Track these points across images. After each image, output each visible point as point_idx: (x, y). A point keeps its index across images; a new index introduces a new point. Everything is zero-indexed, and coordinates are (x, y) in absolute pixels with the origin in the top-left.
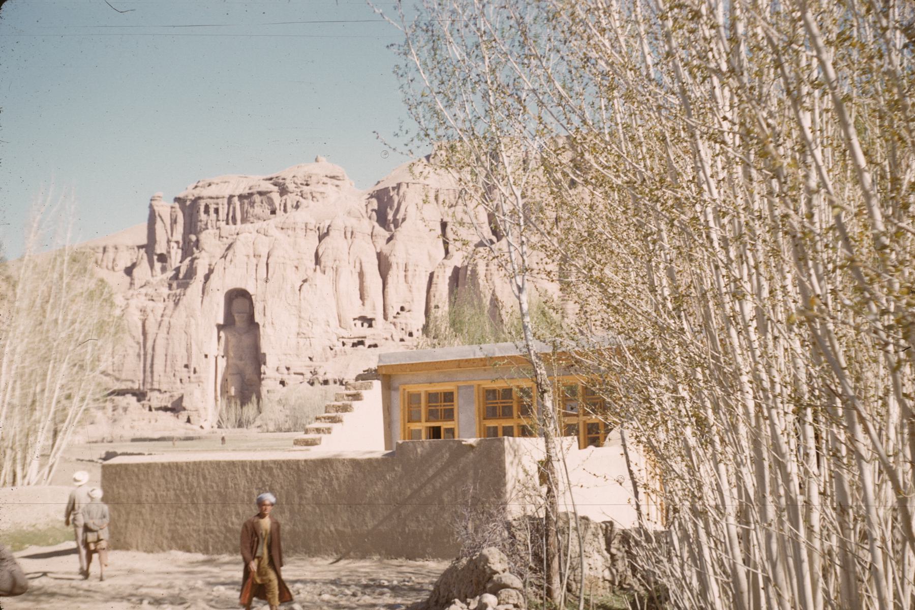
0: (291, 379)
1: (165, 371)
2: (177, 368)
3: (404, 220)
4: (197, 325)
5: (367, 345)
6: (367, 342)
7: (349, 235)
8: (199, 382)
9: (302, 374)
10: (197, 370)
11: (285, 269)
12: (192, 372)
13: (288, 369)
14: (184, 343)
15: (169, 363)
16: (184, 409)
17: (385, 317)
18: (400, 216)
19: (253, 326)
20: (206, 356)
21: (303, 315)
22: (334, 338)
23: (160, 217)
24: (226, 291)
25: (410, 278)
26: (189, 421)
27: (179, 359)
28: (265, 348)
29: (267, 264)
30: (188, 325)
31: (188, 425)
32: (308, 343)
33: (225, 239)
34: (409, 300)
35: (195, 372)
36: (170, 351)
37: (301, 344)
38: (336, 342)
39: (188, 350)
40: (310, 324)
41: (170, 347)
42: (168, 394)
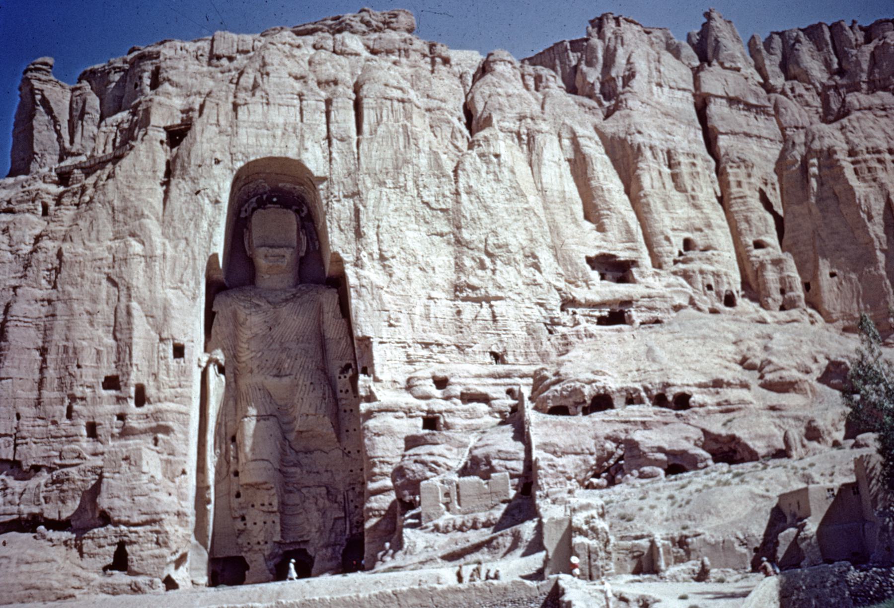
0: (458, 416)
1: (38, 403)
2: (78, 391)
3: (629, 77)
4: (149, 258)
5: (638, 321)
6: (636, 315)
7: (531, 82)
8: (159, 430)
9: (485, 399)
10: (151, 391)
11: (409, 117)
12: (132, 403)
13: (441, 383)
14: (105, 310)
15: (51, 373)
16: (105, 519)
17: (658, 264)
18: (618, 70)
19: (319, 277)
20: (179, 351)
21: (466, 235)
22: (555, 301)
23: (45, 102)
24: (239, 164)
25: (687, 182)
26: (121, 562)
27: (88, 360)
28: (366, 322)
29: (358, 106)
30: (122, 260)
31: (120, 578)
32: (485, 311)
33: (224, 62)
34: (698, 223)
35: (141, 398)
36: (57, 337)
37: (467, 316)
38: (557, 313)
39: (121, 330)
40: (488, 261)
41: (60, 323)
42: (44, 477)
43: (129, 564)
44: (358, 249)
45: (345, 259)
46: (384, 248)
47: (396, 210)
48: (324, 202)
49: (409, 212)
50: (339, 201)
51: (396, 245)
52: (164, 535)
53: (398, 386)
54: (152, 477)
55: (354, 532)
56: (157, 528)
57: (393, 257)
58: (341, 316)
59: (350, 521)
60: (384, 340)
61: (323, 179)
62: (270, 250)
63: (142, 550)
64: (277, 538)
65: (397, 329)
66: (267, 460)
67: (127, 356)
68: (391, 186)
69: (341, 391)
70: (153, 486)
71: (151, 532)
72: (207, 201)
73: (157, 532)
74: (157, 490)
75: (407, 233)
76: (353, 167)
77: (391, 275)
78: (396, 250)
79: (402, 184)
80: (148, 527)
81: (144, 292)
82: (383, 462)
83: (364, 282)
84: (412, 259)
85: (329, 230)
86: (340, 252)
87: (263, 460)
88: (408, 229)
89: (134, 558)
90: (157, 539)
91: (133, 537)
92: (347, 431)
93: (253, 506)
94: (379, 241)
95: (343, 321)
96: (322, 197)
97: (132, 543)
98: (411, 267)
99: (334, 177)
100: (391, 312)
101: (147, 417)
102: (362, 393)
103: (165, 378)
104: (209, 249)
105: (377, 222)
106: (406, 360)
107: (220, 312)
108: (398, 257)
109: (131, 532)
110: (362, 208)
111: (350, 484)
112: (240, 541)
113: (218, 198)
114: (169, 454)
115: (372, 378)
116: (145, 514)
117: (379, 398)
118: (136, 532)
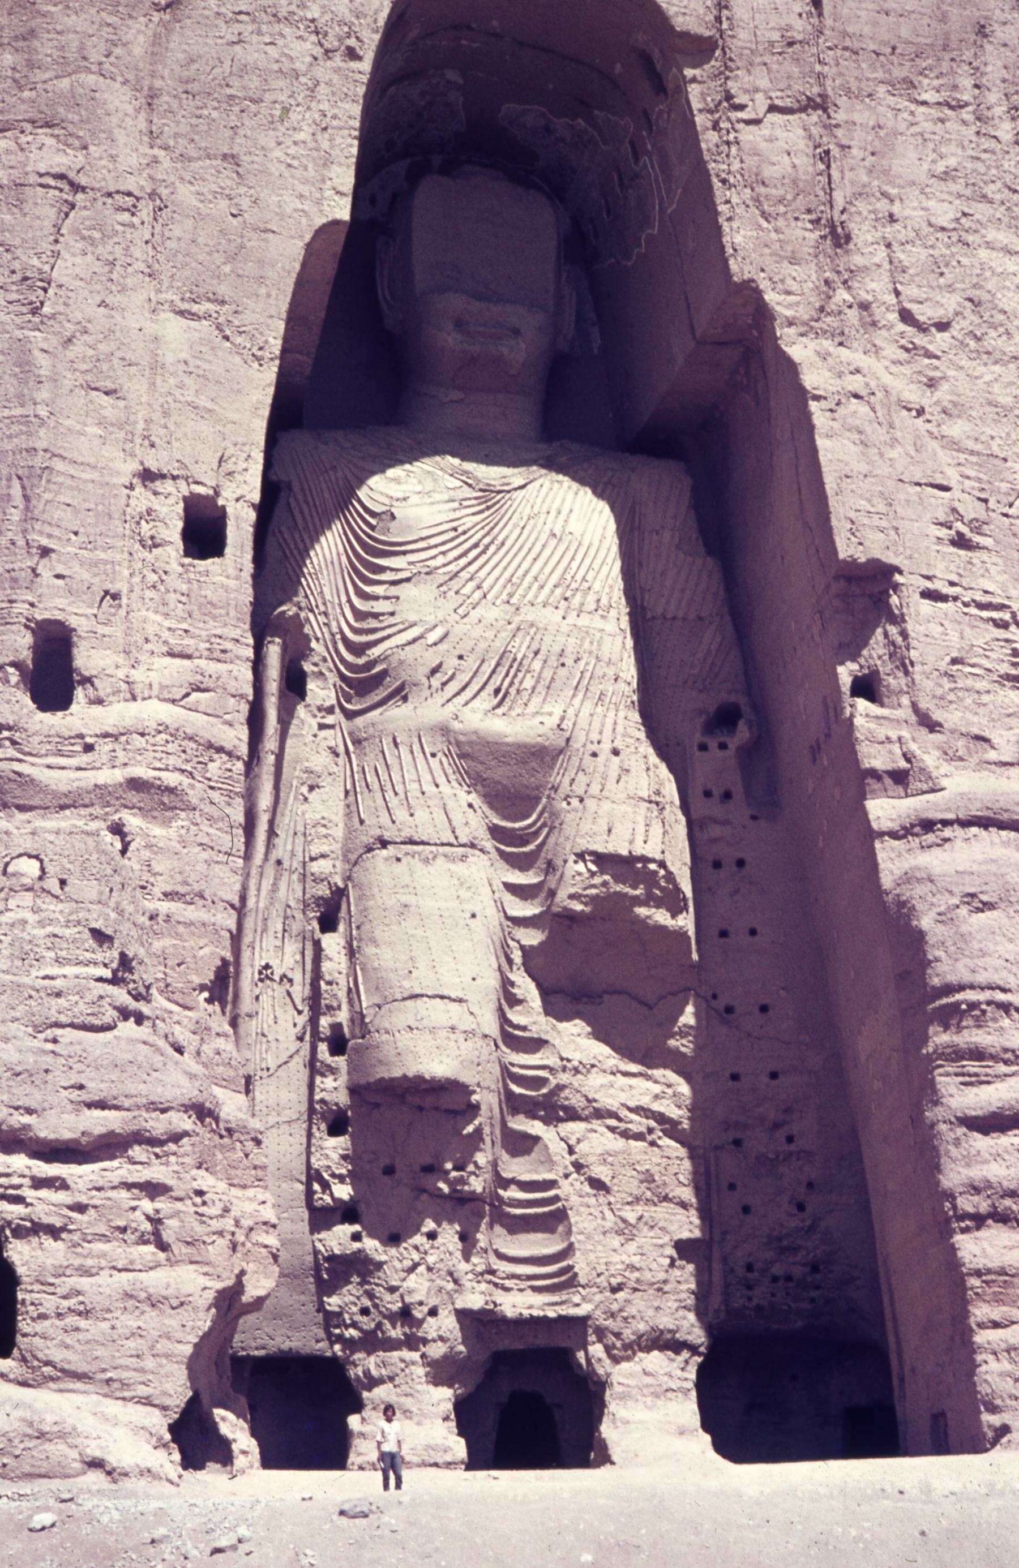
43: (24, 1325)
44: (827, 282)
45: (778, 308)
46: (909, 291)
47: (946, 176)
48: (701, 120)
49: (989, 190)
50: (757, 122)
51: (950, 288)
52: (187, 1207)
53: (992, 755)
54: (125, 962)
55: (738, 1302)
56: (157, 1173)
57: (943, 326)
58: (702, 550)
59: (725, 1259)
61: (701, 48)
62: (476, 306)
63: (86, 1272)
64: (474, 1300)
65: (976, 556)
66: (460, 1001)
67: (15, 515)
68: (929, 96)
69: (708, 794)
70: (121, 995)
71: (129, 1186)
72: (310, 45)
73: (154, 1190)
74: (140, 1019)
75: (983, 253)
76: (799, 24)
77: (932, 384)
78: (949, 304)
79: (966, 97)
80: (117, 1169)
81: (84, 306)
82: (1006, 1008)
83: (855, 383)
84: (993, 340)
85: (721, 208)
86: (764, 285)
87: (442, 997)
88: (989, 245)
89: (50, 1303)
90: (156, 1221)
91: (46, 1205)
92: (723, 934)
93: (389, 1171)
94: (897, 268)
95: (710, 562)
96: (696, 104)
97: (37, 1229)
98: (997, 368)
99: (734, 45)
100: (956, 493)
101: (89, 748)
102: (875, 757)
103: (159, 618)
104: (318, 202)
106: (1005, 668)
107: (296, 487)
108: (955, 330)
109: (39, 1183)
110: (835, 152)
112: (333, 1302)
113: (352, 42)
114: (167, 895)
115: (905, 712)
116: (101, 1105)
117: (944, 782)
118: (58, 1184)
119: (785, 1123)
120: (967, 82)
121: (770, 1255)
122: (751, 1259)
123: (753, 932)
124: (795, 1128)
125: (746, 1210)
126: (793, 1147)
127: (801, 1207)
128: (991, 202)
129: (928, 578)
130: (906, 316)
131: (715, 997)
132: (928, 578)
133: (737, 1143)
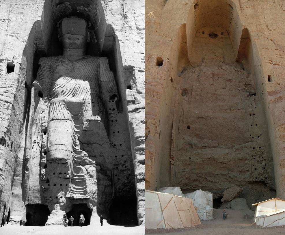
60: (277, 63)
92: (252, 126)
105: (263, 17)
111: (253, 156)
119: (262, 155)
120: (273, 2)
121: (259, 176)
122: (257, 177)
123: (256, 125)
124: (263, 156)
125: (256, 169)
126: (263, 159)
127: (264, 168)
128: (278, 15)
129: (275, 62)
130: (268, 29)
131: (250, 136)
132: (275, 62)
133: (254, 159)
